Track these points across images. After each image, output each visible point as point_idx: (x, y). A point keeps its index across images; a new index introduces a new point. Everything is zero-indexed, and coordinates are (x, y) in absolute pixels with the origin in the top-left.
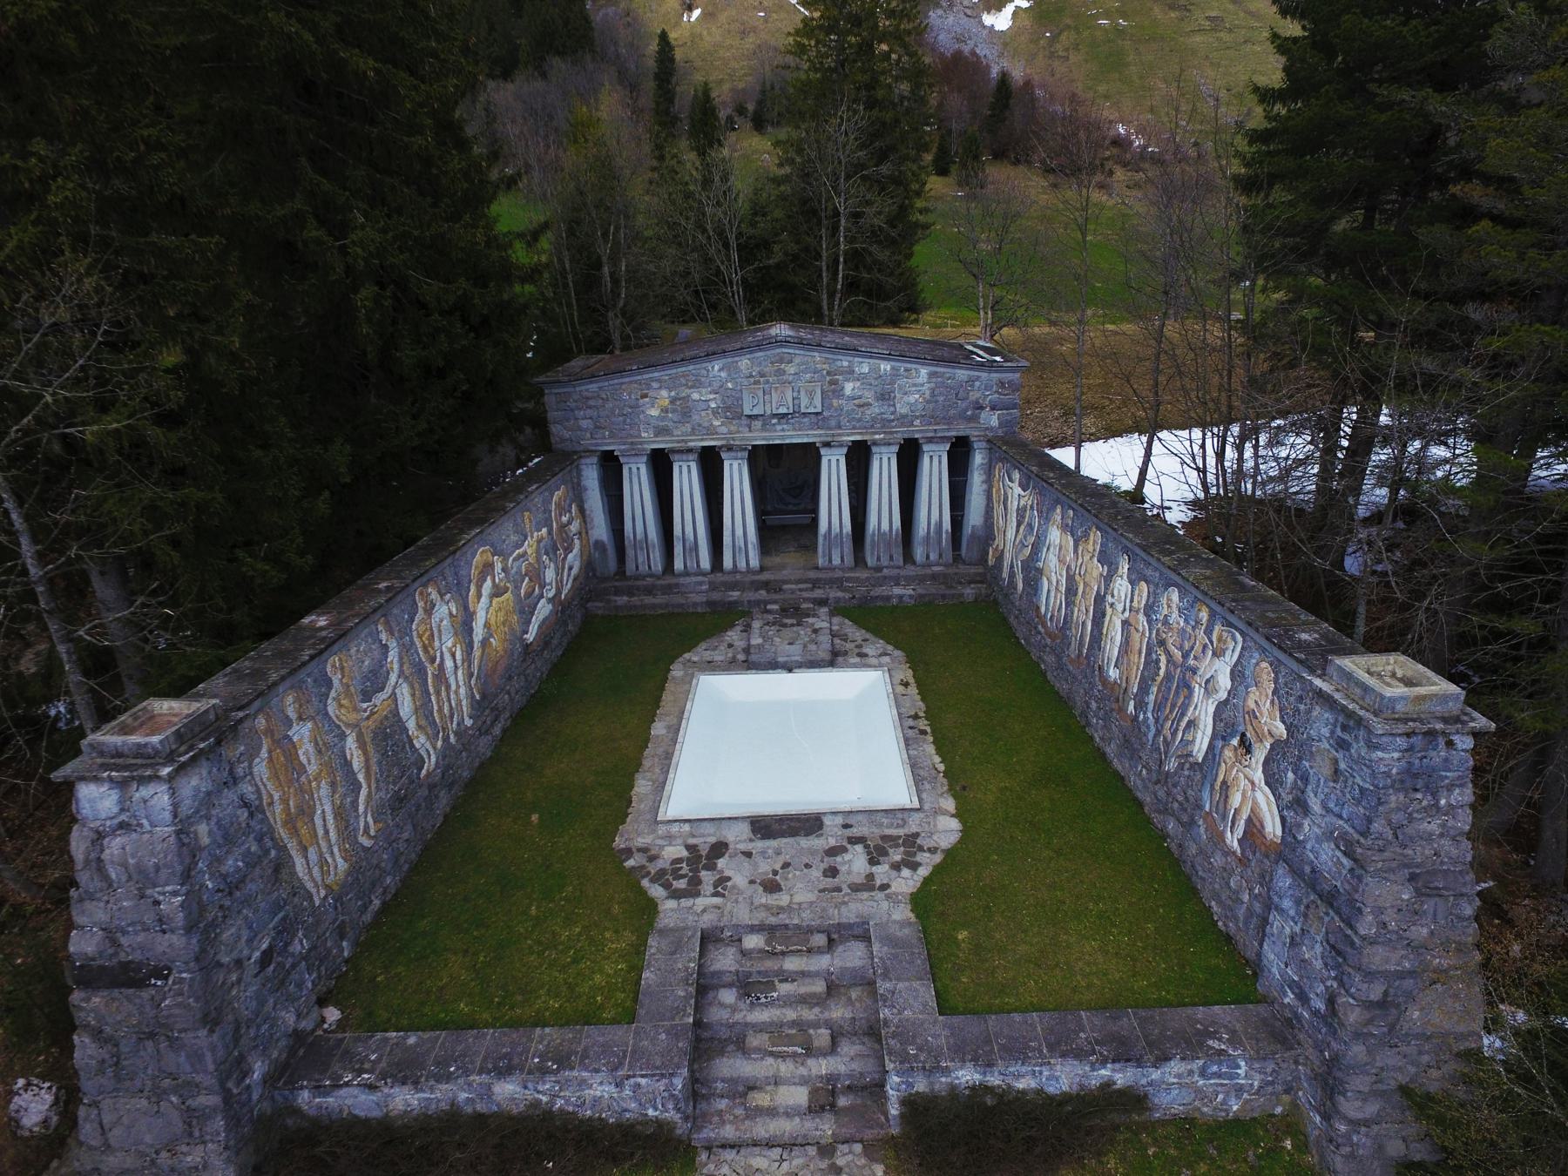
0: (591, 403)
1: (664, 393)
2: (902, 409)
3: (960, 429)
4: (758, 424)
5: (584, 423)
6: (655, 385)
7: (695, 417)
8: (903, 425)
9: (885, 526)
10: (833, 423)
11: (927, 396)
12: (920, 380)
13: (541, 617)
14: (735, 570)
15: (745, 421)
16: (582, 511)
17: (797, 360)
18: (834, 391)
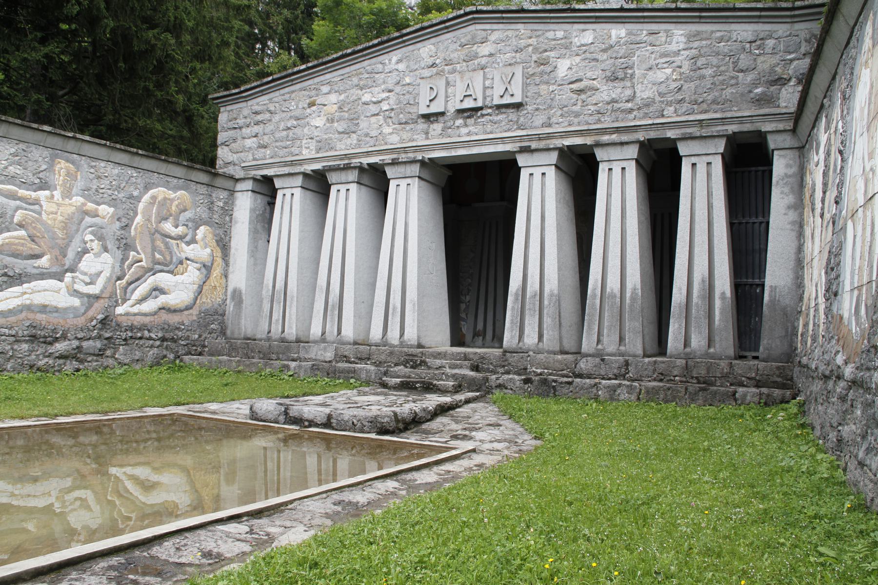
0: (259, 118)
1: (333, 98)
2: (644, 93)
3: (743, 117)
4: (437, 127)
5: (249, 143)
6: (325, 89)
7: (363, 124)
8: (646, 116)
9: (613, 283)
10: (539, 120)
11: (686, 68)
12: (674, 47)
13: (38, 299)
14: (384, 343)
15: (422, 125)
16: (224, 245)
17: (494, 37)
18: (542, 74)
